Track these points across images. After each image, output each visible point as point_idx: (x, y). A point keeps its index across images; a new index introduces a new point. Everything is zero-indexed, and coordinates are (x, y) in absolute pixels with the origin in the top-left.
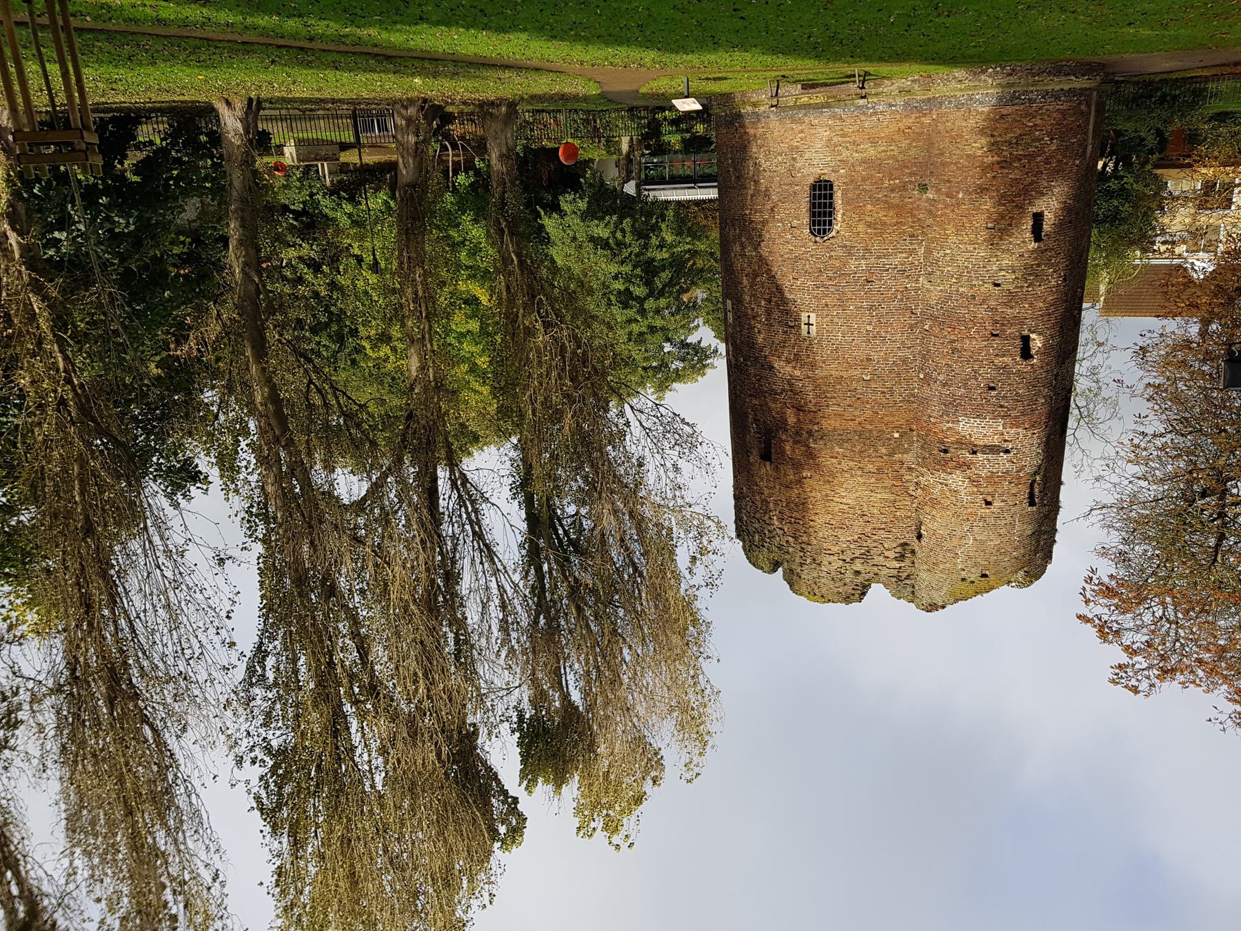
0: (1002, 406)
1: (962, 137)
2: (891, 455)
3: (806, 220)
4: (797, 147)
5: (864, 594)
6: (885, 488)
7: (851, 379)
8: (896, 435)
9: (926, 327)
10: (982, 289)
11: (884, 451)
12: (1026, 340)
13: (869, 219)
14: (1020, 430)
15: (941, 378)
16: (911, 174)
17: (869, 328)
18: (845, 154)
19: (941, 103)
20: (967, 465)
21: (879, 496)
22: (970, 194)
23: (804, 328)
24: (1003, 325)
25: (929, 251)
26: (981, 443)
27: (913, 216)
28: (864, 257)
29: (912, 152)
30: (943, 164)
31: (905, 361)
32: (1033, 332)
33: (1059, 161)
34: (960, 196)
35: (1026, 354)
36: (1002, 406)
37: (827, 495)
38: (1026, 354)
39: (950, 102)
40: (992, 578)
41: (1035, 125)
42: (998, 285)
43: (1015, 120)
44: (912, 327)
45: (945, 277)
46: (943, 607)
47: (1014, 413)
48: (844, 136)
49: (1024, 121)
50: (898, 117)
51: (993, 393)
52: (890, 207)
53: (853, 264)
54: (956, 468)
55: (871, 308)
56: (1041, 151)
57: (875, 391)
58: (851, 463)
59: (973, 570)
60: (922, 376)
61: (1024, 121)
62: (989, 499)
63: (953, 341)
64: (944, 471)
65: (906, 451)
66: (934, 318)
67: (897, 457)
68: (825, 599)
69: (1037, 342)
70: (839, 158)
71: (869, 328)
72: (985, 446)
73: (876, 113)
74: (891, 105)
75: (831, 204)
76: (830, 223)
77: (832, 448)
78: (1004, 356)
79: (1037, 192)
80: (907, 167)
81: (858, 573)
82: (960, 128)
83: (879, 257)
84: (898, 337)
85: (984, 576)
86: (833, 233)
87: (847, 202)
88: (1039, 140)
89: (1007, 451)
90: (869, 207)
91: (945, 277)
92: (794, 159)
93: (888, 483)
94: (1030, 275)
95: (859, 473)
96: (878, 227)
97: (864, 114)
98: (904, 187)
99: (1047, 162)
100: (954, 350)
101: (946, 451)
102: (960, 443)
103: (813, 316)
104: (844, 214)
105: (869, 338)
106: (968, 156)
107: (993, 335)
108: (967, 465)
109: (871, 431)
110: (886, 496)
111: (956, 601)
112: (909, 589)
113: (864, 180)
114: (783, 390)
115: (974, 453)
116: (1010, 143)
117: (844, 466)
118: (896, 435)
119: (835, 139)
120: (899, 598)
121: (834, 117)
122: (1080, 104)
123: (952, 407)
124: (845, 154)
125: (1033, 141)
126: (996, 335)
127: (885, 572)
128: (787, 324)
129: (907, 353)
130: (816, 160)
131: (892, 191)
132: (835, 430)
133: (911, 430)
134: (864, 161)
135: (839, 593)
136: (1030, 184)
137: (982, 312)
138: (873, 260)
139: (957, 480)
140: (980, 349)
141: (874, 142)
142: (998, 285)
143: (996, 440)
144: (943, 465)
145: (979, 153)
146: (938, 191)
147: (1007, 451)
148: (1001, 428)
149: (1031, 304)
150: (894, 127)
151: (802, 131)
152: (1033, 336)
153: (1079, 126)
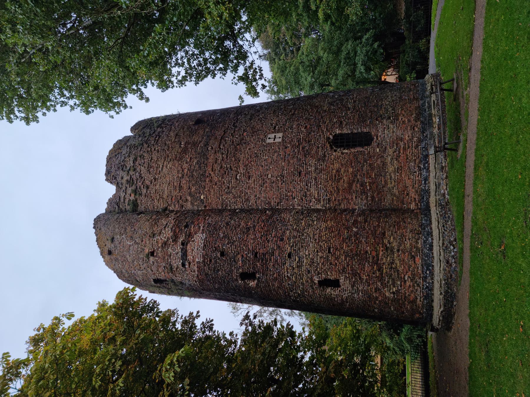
0: (211, 261)
1: (398, 229)
2: (190, 194)
3: (345, 131)
4: (398, 120)
5: (111, 183)
6: (171, 192)
7: (238, 167)
8: (202, 197)
9: (268, 212)
10: (287, 246)
11: (192, 190)
12: (252, 276)
13: (343, 170)
14: (196, 272)
15: (232, 222)
16: (373, 198)
17: (270, 176)
18: (390, 151)
19: (426, 215)
20: (175, 239)
21: (166, 189)
22: (355, 236)
23: (272, 136)
24: (262, 261)
25: (318, 211)
26: (188, 247)
27: (342, 200)
28: (316, 169)
29: (389, 197)
30: (379, 218)
31: (248, 200)
32: (258, 281)
33: (377, 298)
34: (354, 229)
35: (245, 276)
36: (211, 261)
37: (168, 156)
38: (245, 276)
39: (426, 220)
40: (107, 257)
41: (405, 281)
42: (290, 256)
43: (410, 266)
44: (269, 203)
45: (298, 222)
46: (94, 228)
47: (206, 268)
48: (404, 149)
49: (410, 273)
50: (417, 185)
51: (219, 255)
52: (350, 184)
53: (312, 162)
54: (175, 232)
55: (282, 176)
56: (384, 285)
57: (229, 182)
58: (186, 170)
59: (113, 246)
60: (237, 211)
61: (410, 273)
62: (155, 255)
63: (254, 226)
64: (174, 226)
65: (192, 204)
66: (271, 217)
67: (189, 198)
68: (109, 159)
69: (252, 284)
70: (388, 147)
71: (270, 175)
72: (186, 251)
73: (420, 169)
74: (426, 179)
75: (354, 146)
76: (340, 147)
77: (196, 158)
78: (242, 262)
79: (354, 282)
80: (378, 194)
81: (122, 178)
82: (405, 227)
83: (315, 179)
84: (263, 195)
85: (110, 253)
86: (335, 148)
87: (355, 156)
88: (394, 284)
89: (183, 265)
90: (351, 170)
91: (298, 222)
92: (389, 118)
93: (174, 193)
94: (296, 278)
95: (180, 175)
96: (337, 177)
97: (420, 162)
98: (364, 192)
99: (377, 290)
100: (248, 229)
101: (186, 226)
102: (190, 236)
103: (278, 140)
104: (347, 153)
105: (263, 177)
106: (384, 234)
107: (256, 253)
108: (175, 239)
109: (205, 181)
110: (166, 193)
111: (97, 235)
112: (113, 209)
113: (370, 165)
114: (236, 127)
115: (183, 244)
116: (392, 263)
117: (185, 166)
118: (202, 197)
119: (402, 144)
120: (107, 203)
121: (420, 141)
122: (420, 313)
123: (212, 231)
124: (390, 151)
125: (393, 280)
126: (256, 256)
127: (122, 195)
128: (277, 125)
129: (252, 201)
130: (385, 133)
131: (362, 185)
132: (207, 159)
133: (205, 207)
134: (384, 164)
135: (111, 168)
136: (360, 278)
137: (271, 245)
138: (314, 175)
139: (168, 233)
140: (247, 246)
141: (399, 170)
142: (290, 256)
143: (190, 258)
144: (177, 225)
145: (386, 241)
146: (359, 215)
147: (183, 265)
148: (197, 260)
149: (276, 279)
150: (409, 183)
151: (409, 121)
152: (256, 281)
153: (403, 313)
